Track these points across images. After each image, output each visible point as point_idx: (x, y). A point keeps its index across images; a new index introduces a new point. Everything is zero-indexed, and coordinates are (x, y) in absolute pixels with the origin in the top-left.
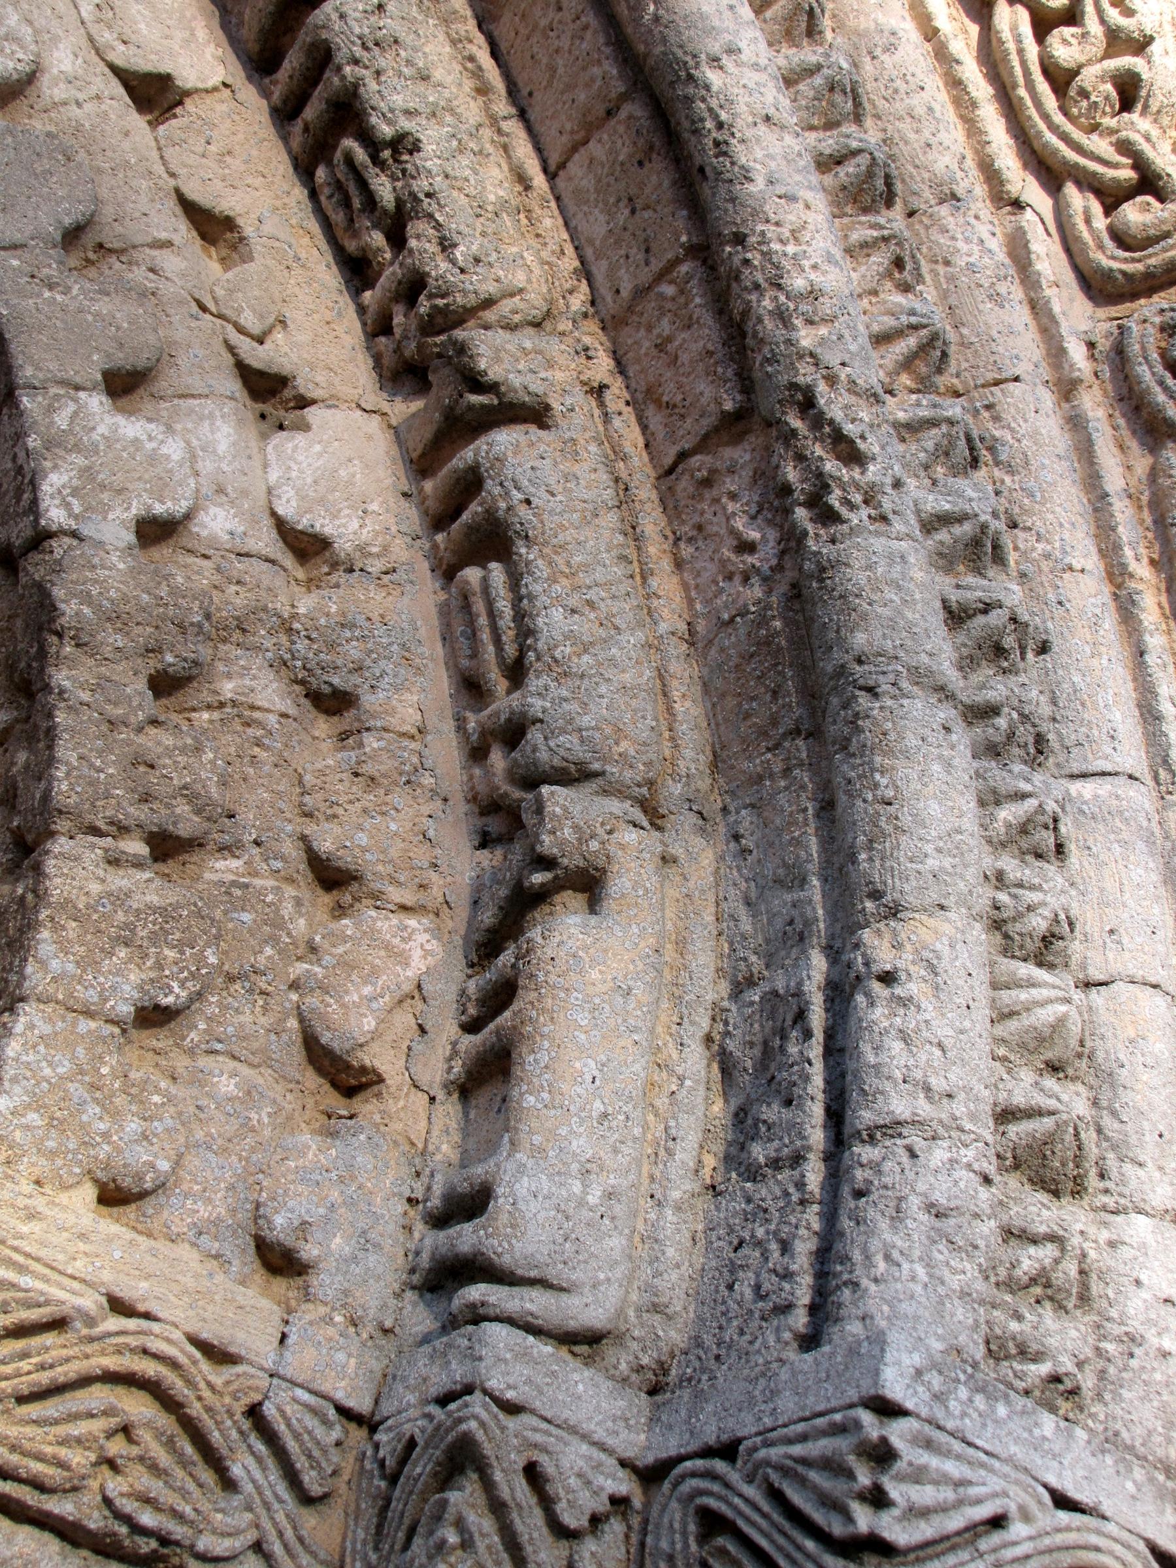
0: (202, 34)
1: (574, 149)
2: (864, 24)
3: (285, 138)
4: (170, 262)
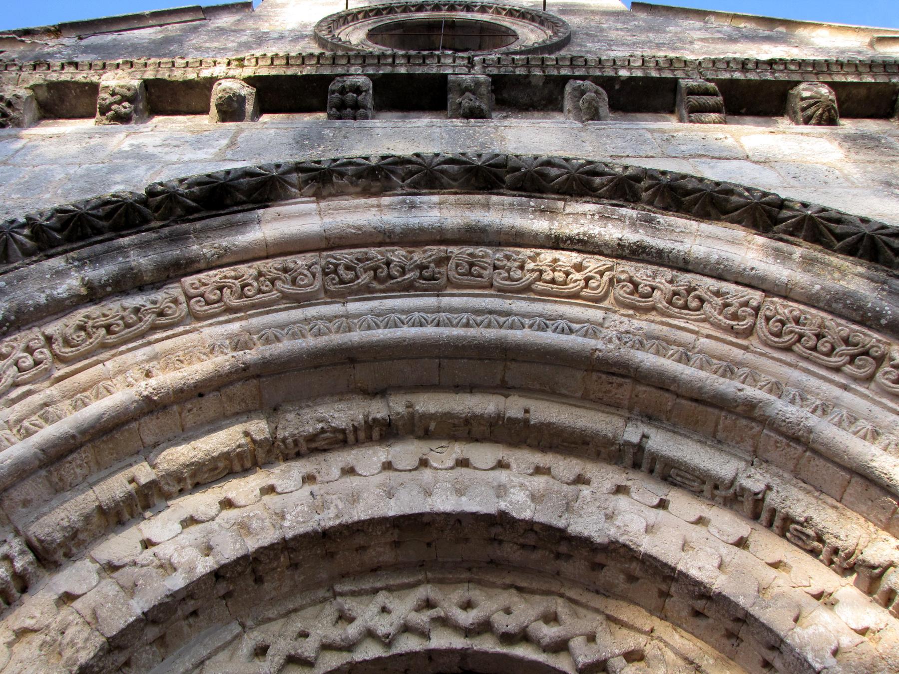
0: (738, 521)
1: (843, 493)
2: (886, 423)
3: (772, 531)
4: (780, 582)
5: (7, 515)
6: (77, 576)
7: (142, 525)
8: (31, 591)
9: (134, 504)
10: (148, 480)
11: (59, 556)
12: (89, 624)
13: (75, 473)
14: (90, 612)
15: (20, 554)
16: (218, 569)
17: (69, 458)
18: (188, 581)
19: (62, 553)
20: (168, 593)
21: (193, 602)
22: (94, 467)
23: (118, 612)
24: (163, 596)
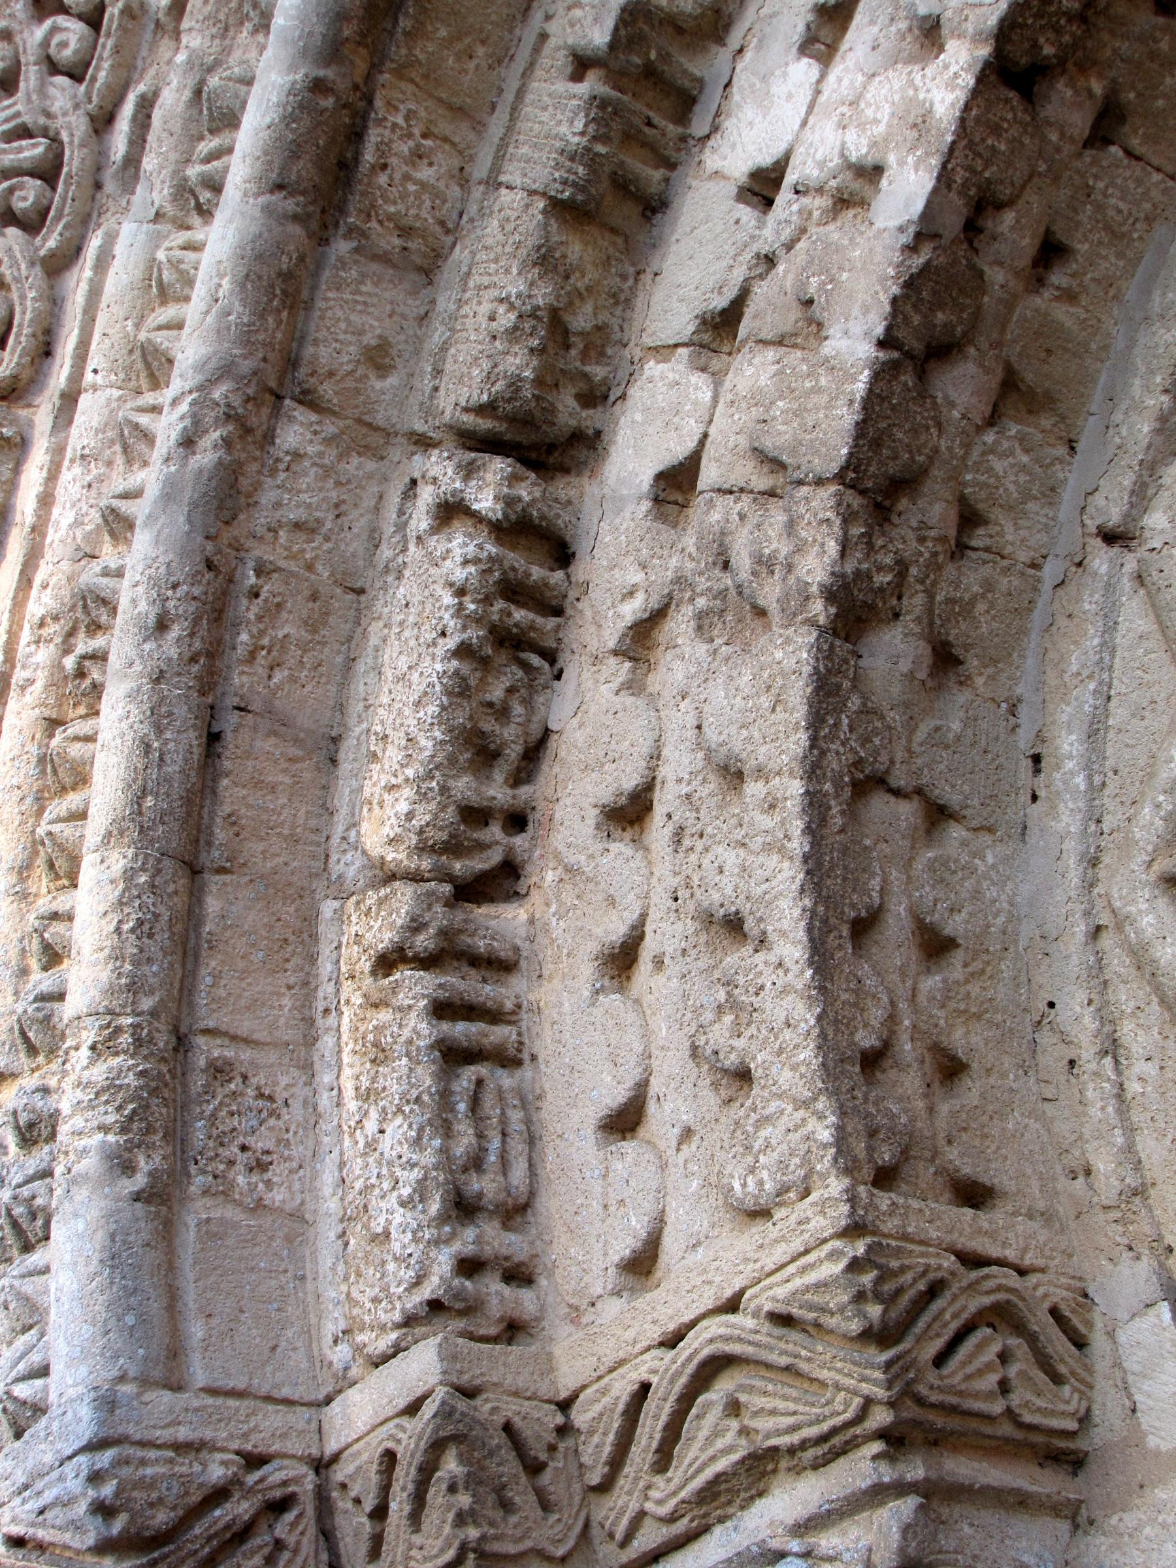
5: (359, 421)
6: (659, 413)
7: (712, 160)
8: (582, 548)
9: (637, 121)
10: (610, 23)
11: (568, 411)
12: (771, 494)
13: (423, 185)
14: (751, 464)
15: (467, 478)
16: (999, 52)
17: (369, 156)
18: (935, 161)
19: (571, 402)
20: (906, 238)
21: (1009, 217)
22: (462, 133)
23: (815, 399)
24: (897, 257)
